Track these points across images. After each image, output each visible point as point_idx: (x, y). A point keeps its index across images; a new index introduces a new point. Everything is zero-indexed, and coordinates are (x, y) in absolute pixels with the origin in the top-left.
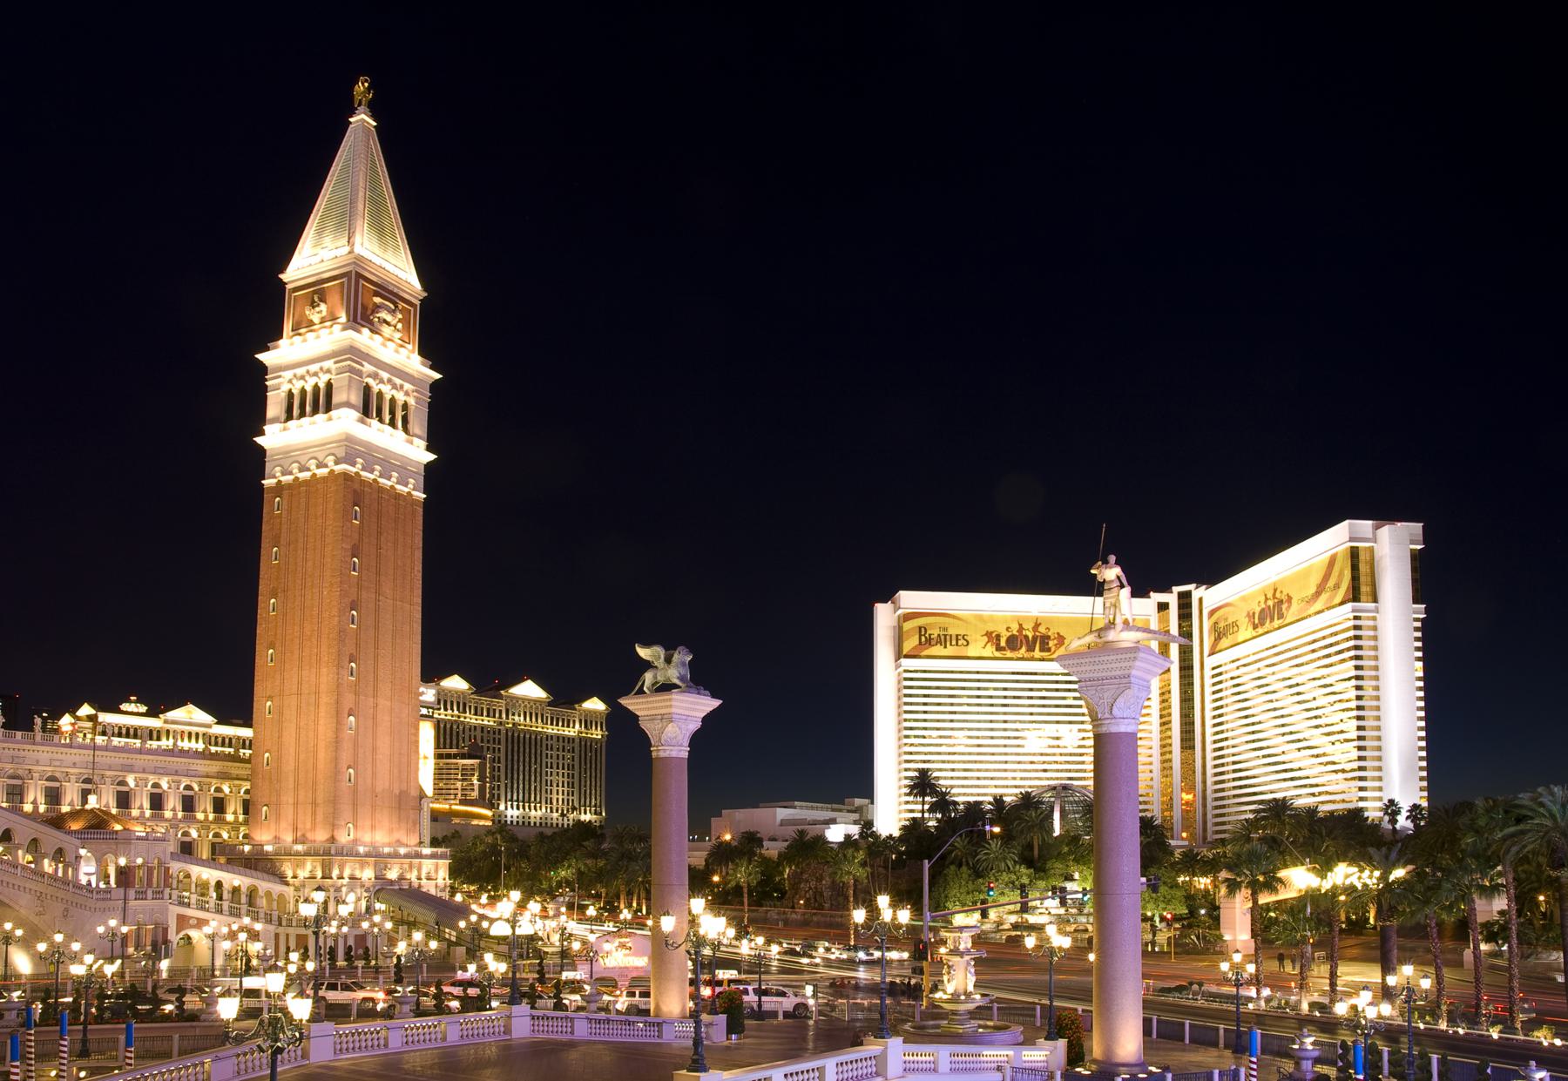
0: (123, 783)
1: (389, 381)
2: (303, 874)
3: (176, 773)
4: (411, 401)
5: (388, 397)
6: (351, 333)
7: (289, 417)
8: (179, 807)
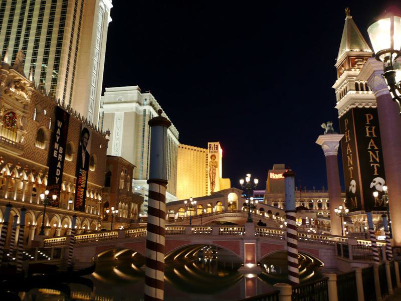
2: (355, 221)
7: (341, 99)
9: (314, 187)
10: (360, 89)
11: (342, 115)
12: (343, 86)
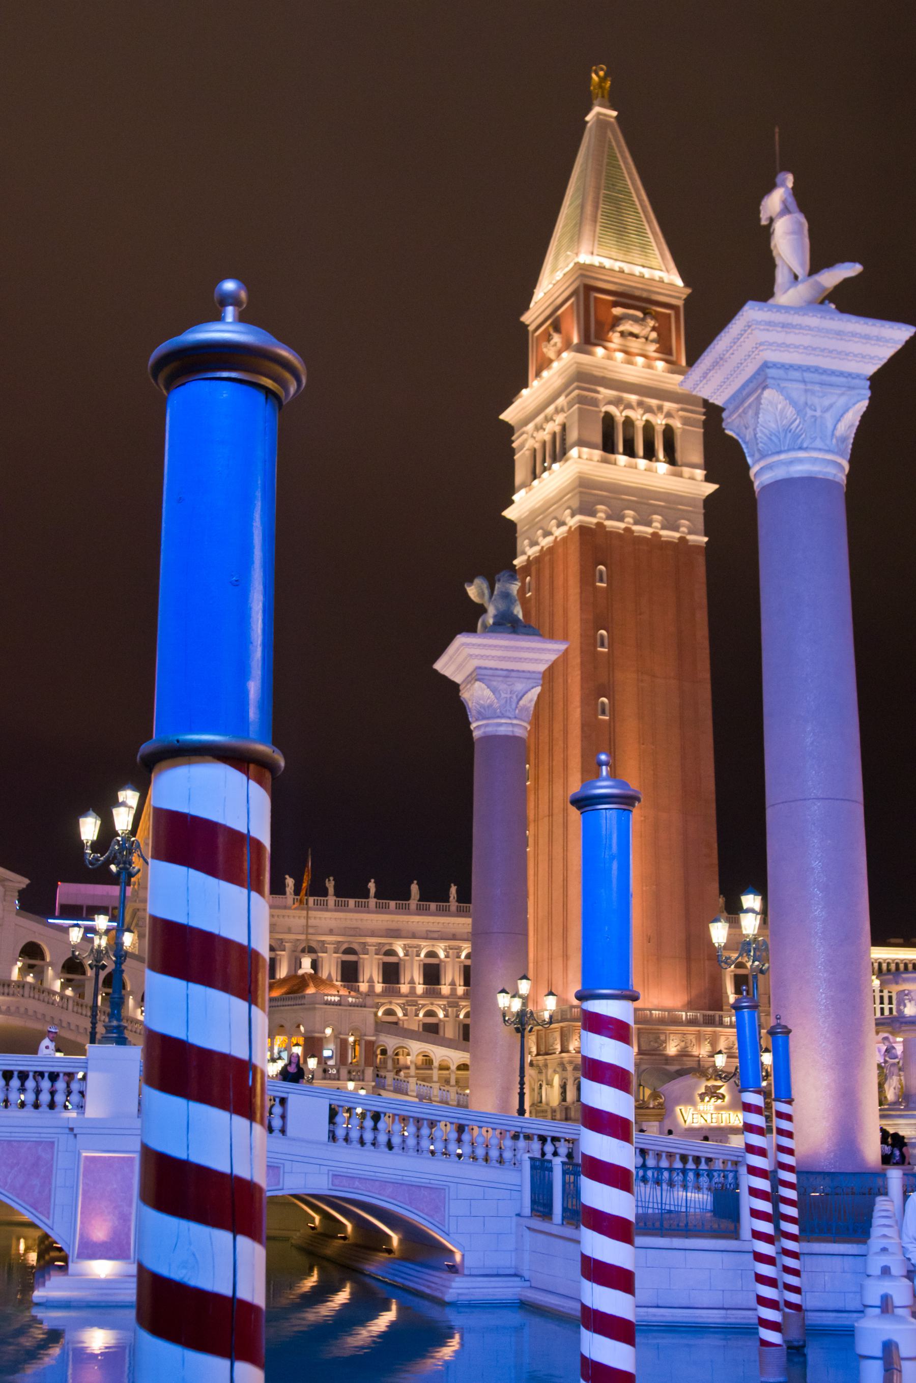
0: (391, 953)
1: (640, 404)
3: (454, 937)
4: (677, 424)
5: (640, 424)
6: (583, 358)
7: (535, 476)
8: (460, 980)
9: (372, 886)
10: (621, 449)
11: (533, 552)
12: (548, 419)
